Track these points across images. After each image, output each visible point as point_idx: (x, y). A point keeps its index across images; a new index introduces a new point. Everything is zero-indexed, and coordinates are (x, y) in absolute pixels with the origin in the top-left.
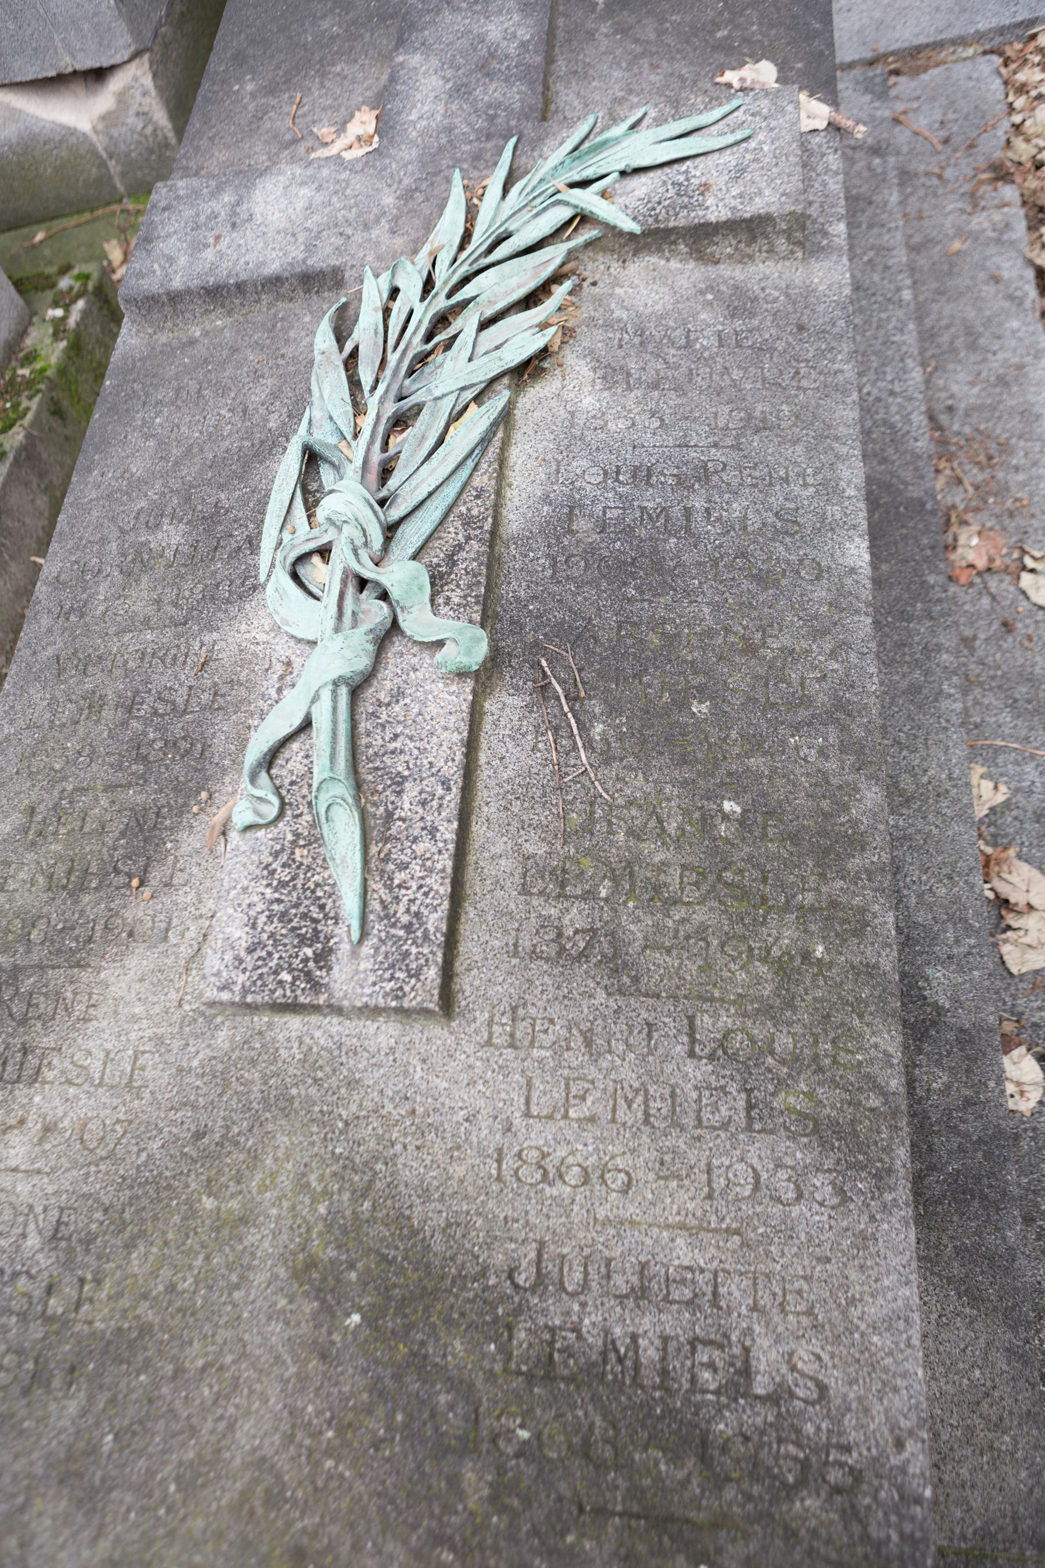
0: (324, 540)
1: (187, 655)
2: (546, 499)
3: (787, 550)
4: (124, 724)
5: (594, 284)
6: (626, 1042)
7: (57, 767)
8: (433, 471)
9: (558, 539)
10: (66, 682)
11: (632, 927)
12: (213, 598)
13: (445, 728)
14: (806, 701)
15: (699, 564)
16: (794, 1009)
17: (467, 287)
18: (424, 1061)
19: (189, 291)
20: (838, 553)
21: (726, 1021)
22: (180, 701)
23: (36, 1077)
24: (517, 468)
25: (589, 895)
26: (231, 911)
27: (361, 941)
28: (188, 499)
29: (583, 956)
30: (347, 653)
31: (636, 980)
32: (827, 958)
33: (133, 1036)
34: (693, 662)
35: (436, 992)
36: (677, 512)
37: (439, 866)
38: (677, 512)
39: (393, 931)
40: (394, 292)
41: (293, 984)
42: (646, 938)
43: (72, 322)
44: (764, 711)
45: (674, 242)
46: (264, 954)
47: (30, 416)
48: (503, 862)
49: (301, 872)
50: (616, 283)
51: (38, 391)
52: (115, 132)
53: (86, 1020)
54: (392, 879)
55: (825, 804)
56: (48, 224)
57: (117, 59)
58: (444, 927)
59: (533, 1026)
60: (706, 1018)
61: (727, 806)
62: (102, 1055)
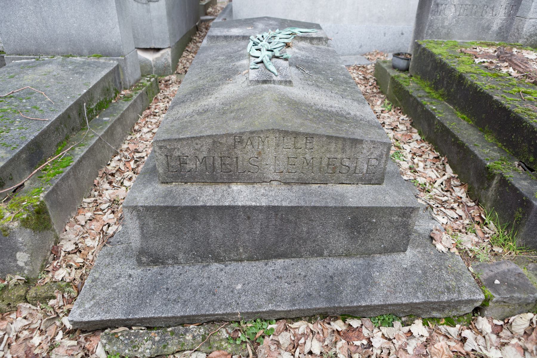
19: (221, 36)
52: (158, 62)
57: (165, 47)
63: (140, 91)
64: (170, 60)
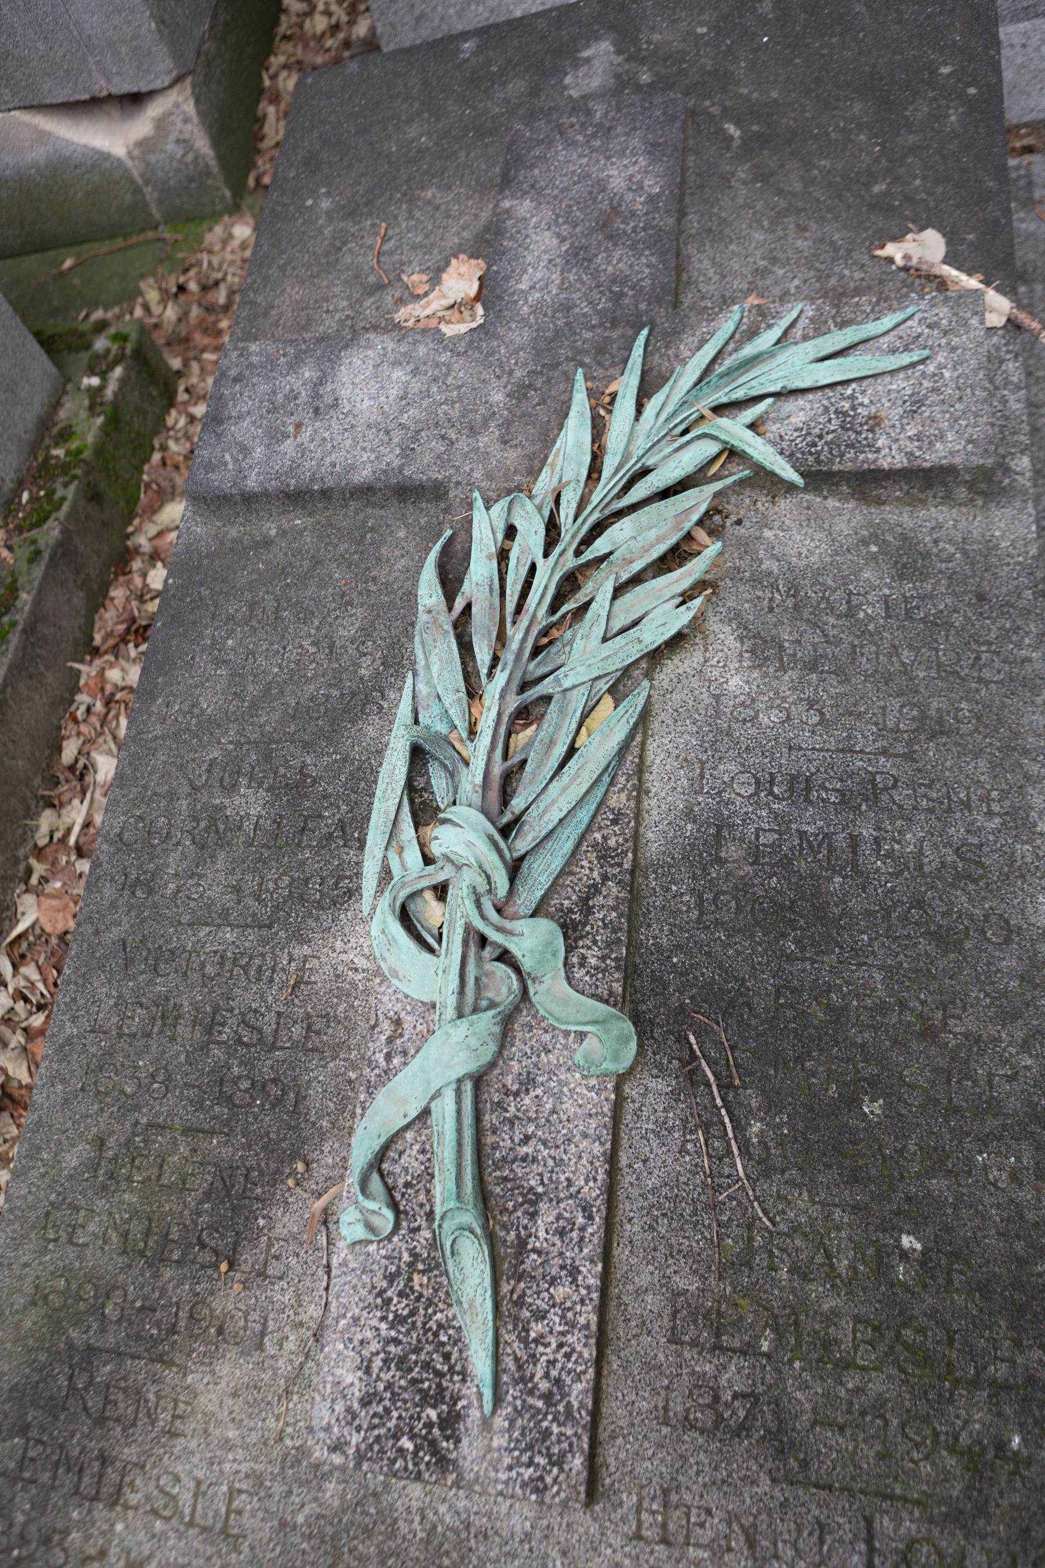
0: (441, 877)
1: (274, 971)
2: (688, 814)
3: (971, 900)
4: (204, 1048)
5: (739, 522)
6: (795, 1545)
7: (129, 1090)
8: (565, 789)
9: (704, 870)
10: (133, 978)
11: (799, 1395)
12: (301, 898)
13: (585, 1136)
14: (994, 1107)
15: (870, 913)
16: (988, 1517)
17: (598, 542)
18: (564, 1554)
19: (266, 494)
20: (1030, 910)
21: (909, 1526)
22: (268, 1030)
23: (115, 1500)
24: (655, 769)
25: (748, 1350)
26: (340, 1346)
27: (494, 1412)
28: (268, 757)
29: (742, 1429)
30: (473, 1042)
31: (805, 1465)
32: (1025, 1453)
33: (227, 1467)
34: (863, 1045)
35: (582, 1489)
36: (841, 840)
37: (582, 1320)
38: (841, 840)
39: (530, 1400)
40: (511, 532)
41: (415, 1453)
42: (814, 1410)
43: (109, 392)
44: (946, 1117)
45: (837, 484)
46: (380, 1409)
47: (65, 507)
48: (649, 1298)
49: (421, 1306)
50: (765, 523)
51: (75, 477)
52: (153, 159)
53: (174, 1435)
54: (527, 1331)
55: (1019, 1246)
56: (77, 249)
57: (158, 84)
58: (589, 1402)
59: (688, 1515)
60: (886, 1521)
61: (906, 1241)
62: (192, 1485)
63: (51, 533)
64: (203, 145)
